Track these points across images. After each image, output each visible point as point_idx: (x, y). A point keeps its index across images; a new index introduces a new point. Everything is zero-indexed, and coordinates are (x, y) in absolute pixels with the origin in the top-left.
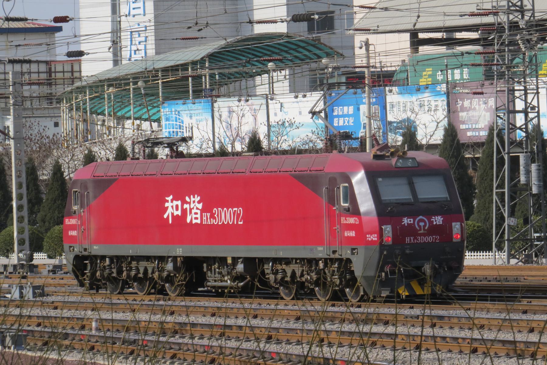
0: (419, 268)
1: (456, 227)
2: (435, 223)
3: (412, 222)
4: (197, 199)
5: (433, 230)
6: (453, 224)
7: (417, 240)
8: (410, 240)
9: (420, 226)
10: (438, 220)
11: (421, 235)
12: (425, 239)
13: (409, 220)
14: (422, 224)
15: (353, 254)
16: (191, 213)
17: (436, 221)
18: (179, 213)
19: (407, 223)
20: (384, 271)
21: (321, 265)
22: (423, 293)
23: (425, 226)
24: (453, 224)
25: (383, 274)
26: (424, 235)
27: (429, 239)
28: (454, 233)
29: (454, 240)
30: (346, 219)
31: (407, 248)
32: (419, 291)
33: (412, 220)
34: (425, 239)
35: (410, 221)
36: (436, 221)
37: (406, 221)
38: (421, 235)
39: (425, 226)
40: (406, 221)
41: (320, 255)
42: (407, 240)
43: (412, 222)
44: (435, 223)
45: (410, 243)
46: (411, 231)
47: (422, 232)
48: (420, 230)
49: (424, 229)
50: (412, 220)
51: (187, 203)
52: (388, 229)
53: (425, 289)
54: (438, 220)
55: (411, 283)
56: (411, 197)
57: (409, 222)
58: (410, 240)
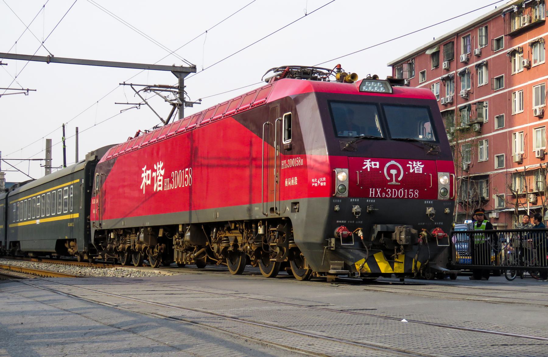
0: (388, 234)
1: (443, 179)
2: (411, 171)
3: (378, 167)
4: (161, 165)
5: (410, 181)
6: (439, 174)
7: (387, 193)
9: (390, 175)
10: (417, 167)
13: (373, 163)
14: (394, 172)
15: (293, 210)
16: (157, 181)
17: (413, 168)
18: (149, 182)
19: (371, 168)
20: (333, 237)
21: (261, 231)
23: (398, 175)
24: (439, 174)
25: (333, 241)
26: (398, 187)
29: (440, 198)
30: (287, 163)
35: (375, 165)
36: (413, 168)
37: (368, 164)
38: (392, 187)
39: (398, 175)
40: (368, 164)
41: (258, 217)
42: (372, 192)
43: (378, 167)
44: (411, 171)
45: (375, 197)
46: (376, 179)
47: (394, 182)
48: (391, 180)
49: (397, 181)
50: (378, 163)
51: (156, 171)
52: (342, 176)
53: (396, 265)
54: (417, 167)
57: (373, 167)
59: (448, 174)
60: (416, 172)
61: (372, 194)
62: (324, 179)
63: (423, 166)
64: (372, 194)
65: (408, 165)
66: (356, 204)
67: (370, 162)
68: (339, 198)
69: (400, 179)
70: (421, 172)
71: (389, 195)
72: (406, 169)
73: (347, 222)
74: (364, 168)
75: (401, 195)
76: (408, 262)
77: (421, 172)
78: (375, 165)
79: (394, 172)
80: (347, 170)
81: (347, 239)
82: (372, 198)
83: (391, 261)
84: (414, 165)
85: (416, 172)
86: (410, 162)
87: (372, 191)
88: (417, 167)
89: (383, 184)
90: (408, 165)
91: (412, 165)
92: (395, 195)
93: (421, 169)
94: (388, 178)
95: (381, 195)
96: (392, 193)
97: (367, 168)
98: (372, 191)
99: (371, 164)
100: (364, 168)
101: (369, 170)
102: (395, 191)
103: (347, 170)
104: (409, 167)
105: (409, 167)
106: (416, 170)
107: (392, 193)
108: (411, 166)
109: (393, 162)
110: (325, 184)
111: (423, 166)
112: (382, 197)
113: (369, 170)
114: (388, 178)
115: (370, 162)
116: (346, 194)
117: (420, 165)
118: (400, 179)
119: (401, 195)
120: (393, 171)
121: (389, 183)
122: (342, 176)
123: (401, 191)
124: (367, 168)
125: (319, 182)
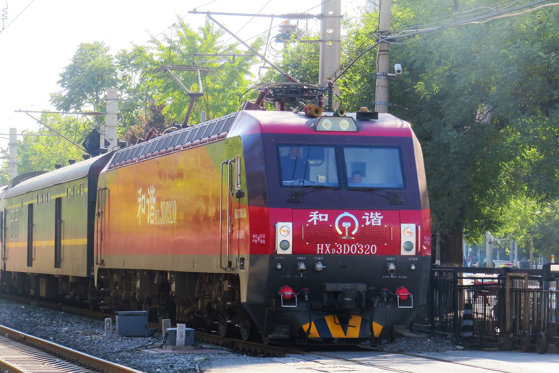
1: (408, 233)
2: (368, 223)
3: (326, 219)
5: (366, 235)
7: (337, 249)
8: (325, 249)
10: (375, 219)
11: (343, 242)
12: (350, 249)
13: (321, 215)
14: (346, 225)
17: (370, 220)
19: (318, 221)
22: (344, 337)
26: (350, 242)
28: (403, 240)
29: (403, 252)
31: (317, 262)
32: (336, 332)
33: (326, 215)
34: (350, 249)
35: (323, 217)
36: (370, 220)
37: (315, 217)
39: (351, 229)
42: (320, 248)
43: (326, 219)
44: (368, 223)
45: (324, 254)
46: (326, 234)
48: (344, 234)
50: (326, 215)
52: (284, 232)
54: (375, 219)
55: (326, 318)
57: (321, 220)
58: (325, 249)
60: (373, 224)
61: (320, 250)
62: (264, 236)
63: (381, 217)
64: (320, 250)
65: (363, 217)
67: (317, 214)
69: (354, 233)
70: (379, 224)
71: (339, 251)
74: (309, 221)
75: (354, 251)
76: (366, 324)
77: (379, 224)
78: (323, 217)
80: (290, 225)
83: (344, 324)
84: (372, 217)
85: (373, 224)
86: (366, 214)
87: (320, 247)
88: (375, 219)
89: (334, 239)
90: (363, 217)
91: (369, 216)
92: (346, 251)
93: (380, 221)
95: (331, 251)
96: (343, 248)
98: (320, 247)
99: (318, 217)
100: (309, 221)
101: (315, 223)
102: (347, 247)
103: (290, 225)
104: (365, 219)
105: (365, 219)
107: (343, 248)
108: (367, 218)
109: (346, 214)
110: (264, 241)
111: (381, 217)
112: (331, 254)
113: (315, 223)
115: (317, 214)
116: (289, 251)
117: (379, 216)
119: (354, 251)
120: (345, 223)
122: (284, 232)
123: (354, 247)
125: (259, 239)
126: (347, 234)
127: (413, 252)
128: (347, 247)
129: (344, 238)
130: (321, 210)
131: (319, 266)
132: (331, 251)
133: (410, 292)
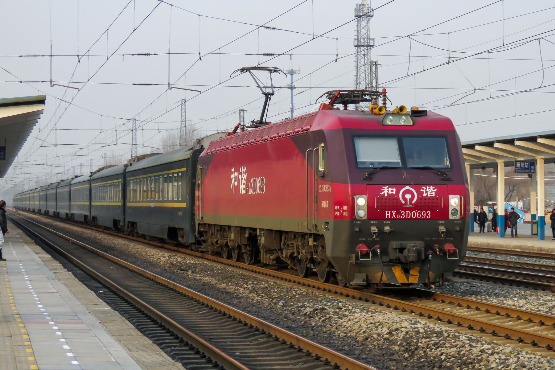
1: (454, 201)
2: (425, 195)
3: (394, 193)
5: (423, 204)
6: (450, 196)
7: (401, 215)
9: (405, 199)
10: (430, 191)
11: (405, 209)
13: (390, 189)
14: (408, 196)
17: (426, 192)
19: (388, 194)
22: (406, 281)
23: (412, 199)
24: (450, 196)
26: (411, 210)
27: (415, 214)
29: (451, 217)
31: (386, 225)
33: (394, 190)
35: (392, 191)
36: (426, 192)
37: (386, 191)
40: (386, 191)
42: (388, 214)
44: (425, 195)
45: (391, 219)
47: (409, 205)
48: (406, 203)
49: (411, 203)
50: (394, 190)
52: (361, 201)
54: (430, 191)
56: (399, 161)
57: (390, 193)
59: (458, 196)
60: (429, 196)
61: (388, 216)
63: (435, 190)
64: (388, 216)
65: (422, 190)
66: (373, 225)
68: (359, 220)
69: (413, 202)
70: (434, 196)
71: (403, 216)
72: (420, 194)
73: (367, 240)
74: (382, 194)
75: (414, 216)
77: (434, 196)
78: (392, 191)
79: (408, 196)
81: (366, 255)
82: (388, 219)
83: (406, 271)
84: (428, 190)
85: (429, 196)
86: (424, 188)
87: (388, 213)
88: (430, 192)
89: (398, 207)
90: (422, 190)
91: (426, 189)
93: (434, 193)
94: (404, 202)
95: (396, 216)
96: (405, 214)
97: (384, 194)
98: (388, 213)
100: (382, 194)
101: (386, 195)
102: (408, 213)
103: (365, 196)
106: (429, 194)
107: (405, 214)
108: (424, 191)
109: (407, 188)
111: (435, 190)
112: (397, 219)
113: (386, 195)
114: (404, 202)
118: (413, 202)
119: (414, 216)
120: (408, 195)
121: (404, 206)
122: (361, 201)
124: (384, 194)
126: (408, 203)
127: (458, 217)
128: (408, 213)
129: (407, 206)
130: (391, 185)
131: (387, 228)
132: (396, 216)
133: (455, 247)
